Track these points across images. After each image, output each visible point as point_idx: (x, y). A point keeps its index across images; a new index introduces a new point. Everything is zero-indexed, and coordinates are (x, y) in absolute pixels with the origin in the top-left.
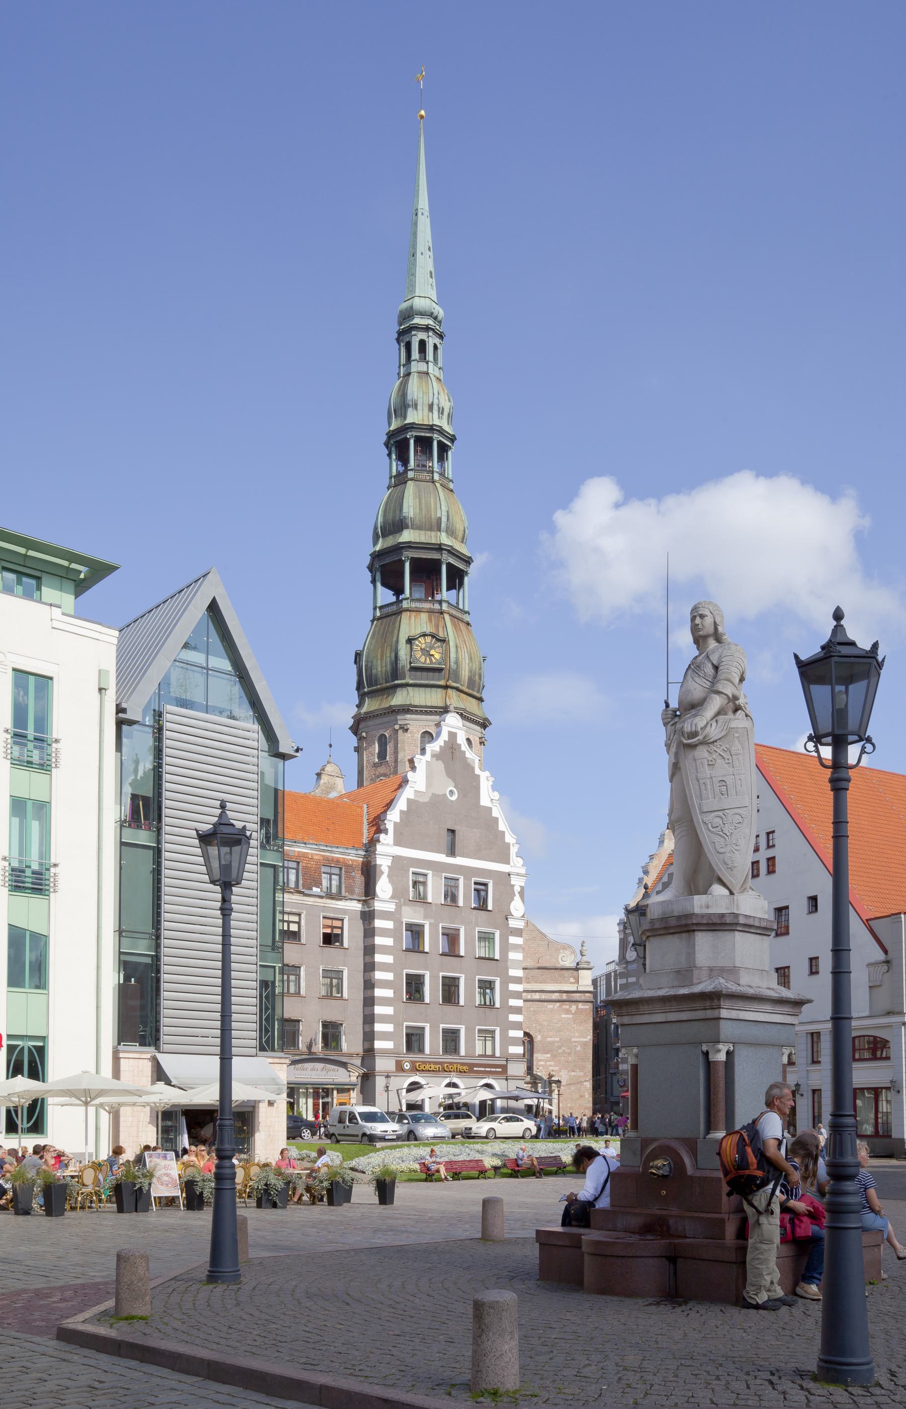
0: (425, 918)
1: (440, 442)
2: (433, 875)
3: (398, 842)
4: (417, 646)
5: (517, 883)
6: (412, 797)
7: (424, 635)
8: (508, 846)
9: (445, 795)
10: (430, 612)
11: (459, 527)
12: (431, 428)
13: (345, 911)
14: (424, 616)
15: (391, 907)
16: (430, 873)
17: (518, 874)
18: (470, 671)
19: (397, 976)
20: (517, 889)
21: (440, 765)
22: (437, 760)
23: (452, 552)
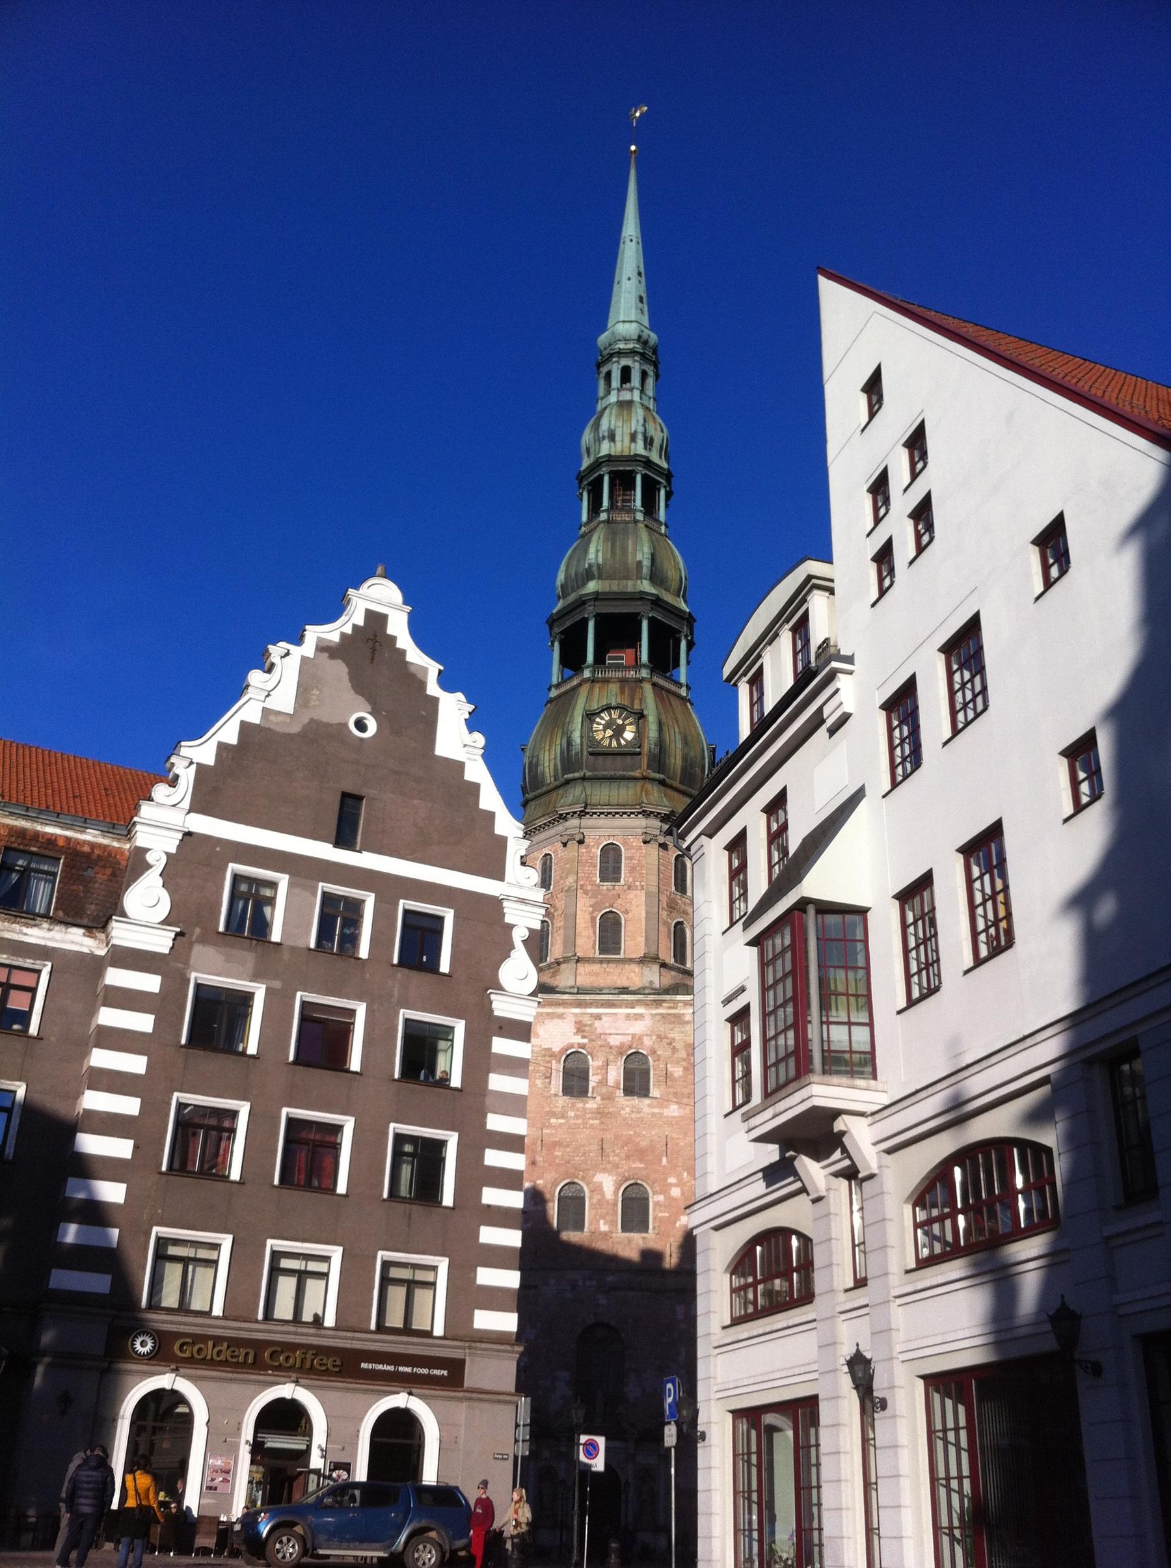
0: (256, 977)
1: (644, 477)
2: (291, 885)
3: (202, 803)
4: (599, 724)
5: (523, 920)
6: (255, 718)
7: (608, 708)
8: (502, 841)
9: (346, 725)
10: (623, 681)
11: (671, 574)
12: (635, 459)
13: (44, 952)
14: (614, 688)
15: (161, 942)
16: (283, 880)
17: (522, 901)
18: (685, 759)
19: (153, 1108)
20: (519, 936)
21: (339, 670)
22: (332, 657)
23: (657, 602)
